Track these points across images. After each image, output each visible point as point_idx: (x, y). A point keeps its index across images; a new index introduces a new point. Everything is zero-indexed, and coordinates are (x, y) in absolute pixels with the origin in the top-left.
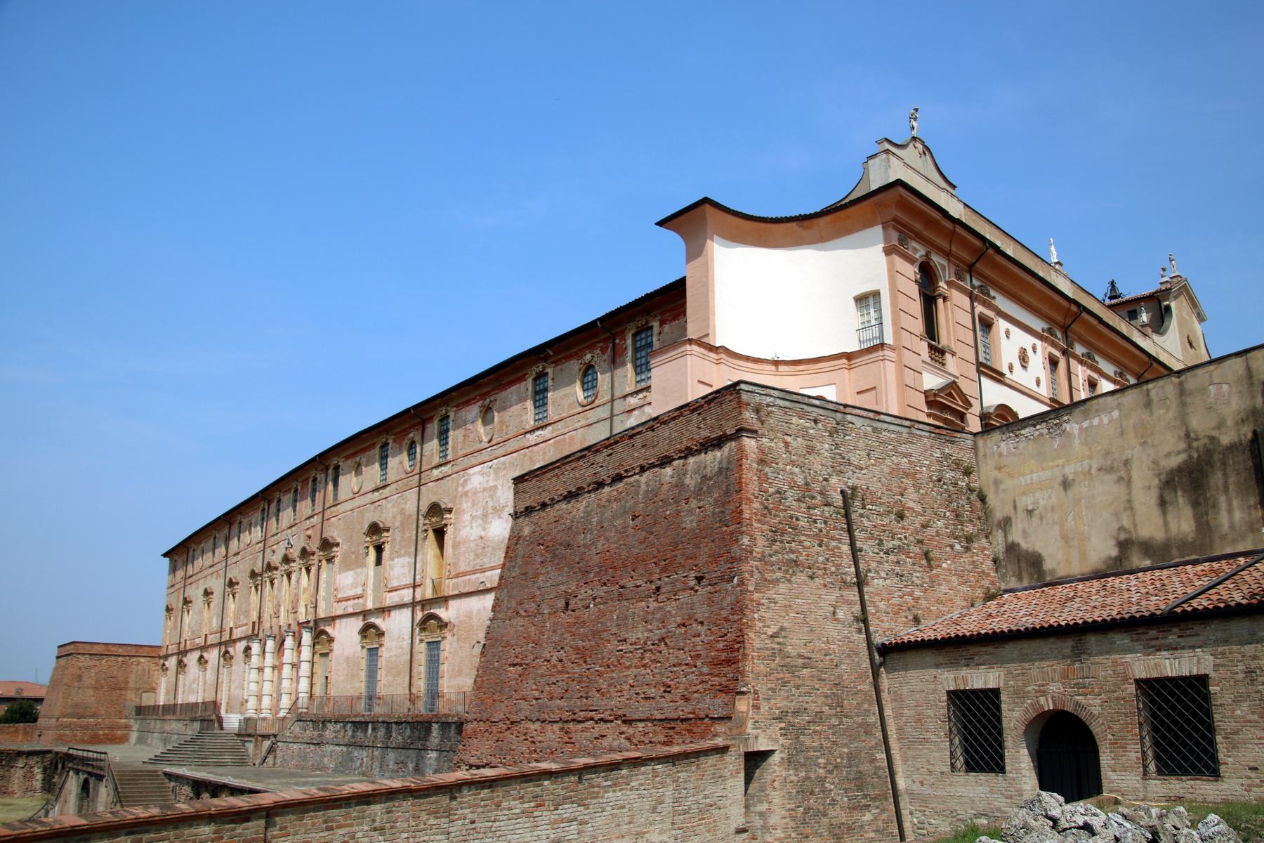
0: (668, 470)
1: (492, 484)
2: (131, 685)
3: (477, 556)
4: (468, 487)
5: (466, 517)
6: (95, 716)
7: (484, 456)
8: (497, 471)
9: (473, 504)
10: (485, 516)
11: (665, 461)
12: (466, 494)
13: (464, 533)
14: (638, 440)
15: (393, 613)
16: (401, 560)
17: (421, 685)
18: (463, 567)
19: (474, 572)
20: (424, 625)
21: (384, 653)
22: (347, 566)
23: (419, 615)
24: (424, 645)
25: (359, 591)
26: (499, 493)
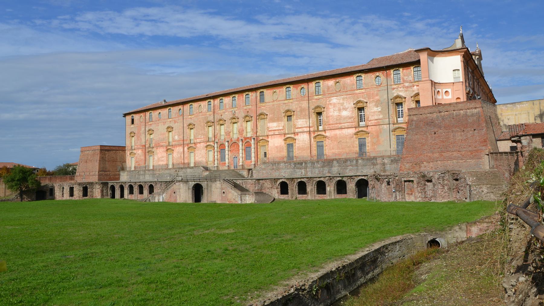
0: (462, 112)
1: (341, 102)
2: (118, 160)
3: (337, 120)
4: (331, 102)
5: (332, 110)
6: (109, 171)
7: (337, 94)
8: (343, 99)
9: (334, 107)
10: (340, 110)
11: (462, 110)
12: (331, 104)
13: (331, 114)
14: (452, 106)
15: (299, 134)
16: (302, 120)
17: (315, 152)
18: (331, 122)
19: (337, 124)
20: (315, 137)
21: (297, 145)
22: (273, 120)
23: (313, 135)
24: (315, 143)
25: (281, 128)
26: (345, 104)
